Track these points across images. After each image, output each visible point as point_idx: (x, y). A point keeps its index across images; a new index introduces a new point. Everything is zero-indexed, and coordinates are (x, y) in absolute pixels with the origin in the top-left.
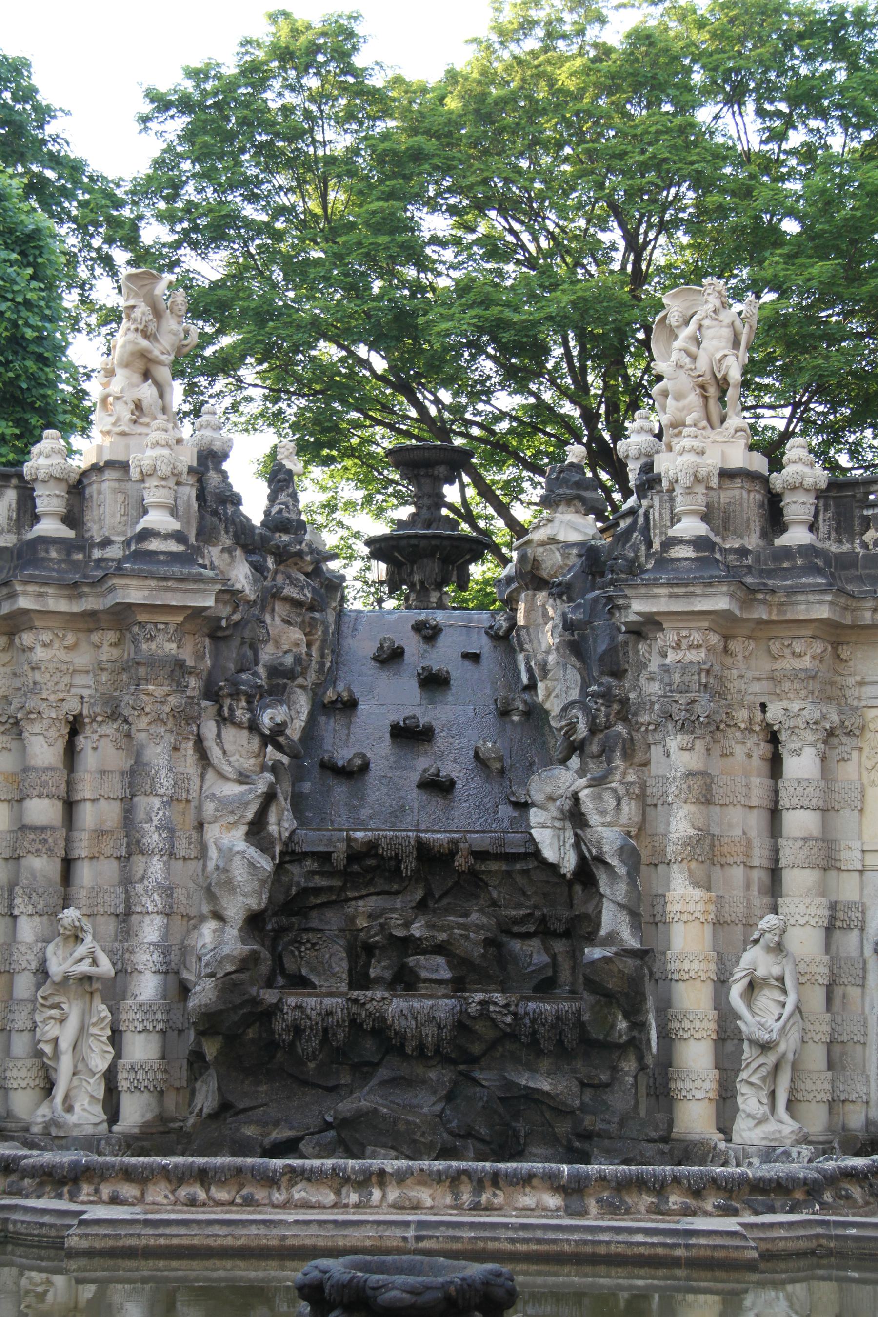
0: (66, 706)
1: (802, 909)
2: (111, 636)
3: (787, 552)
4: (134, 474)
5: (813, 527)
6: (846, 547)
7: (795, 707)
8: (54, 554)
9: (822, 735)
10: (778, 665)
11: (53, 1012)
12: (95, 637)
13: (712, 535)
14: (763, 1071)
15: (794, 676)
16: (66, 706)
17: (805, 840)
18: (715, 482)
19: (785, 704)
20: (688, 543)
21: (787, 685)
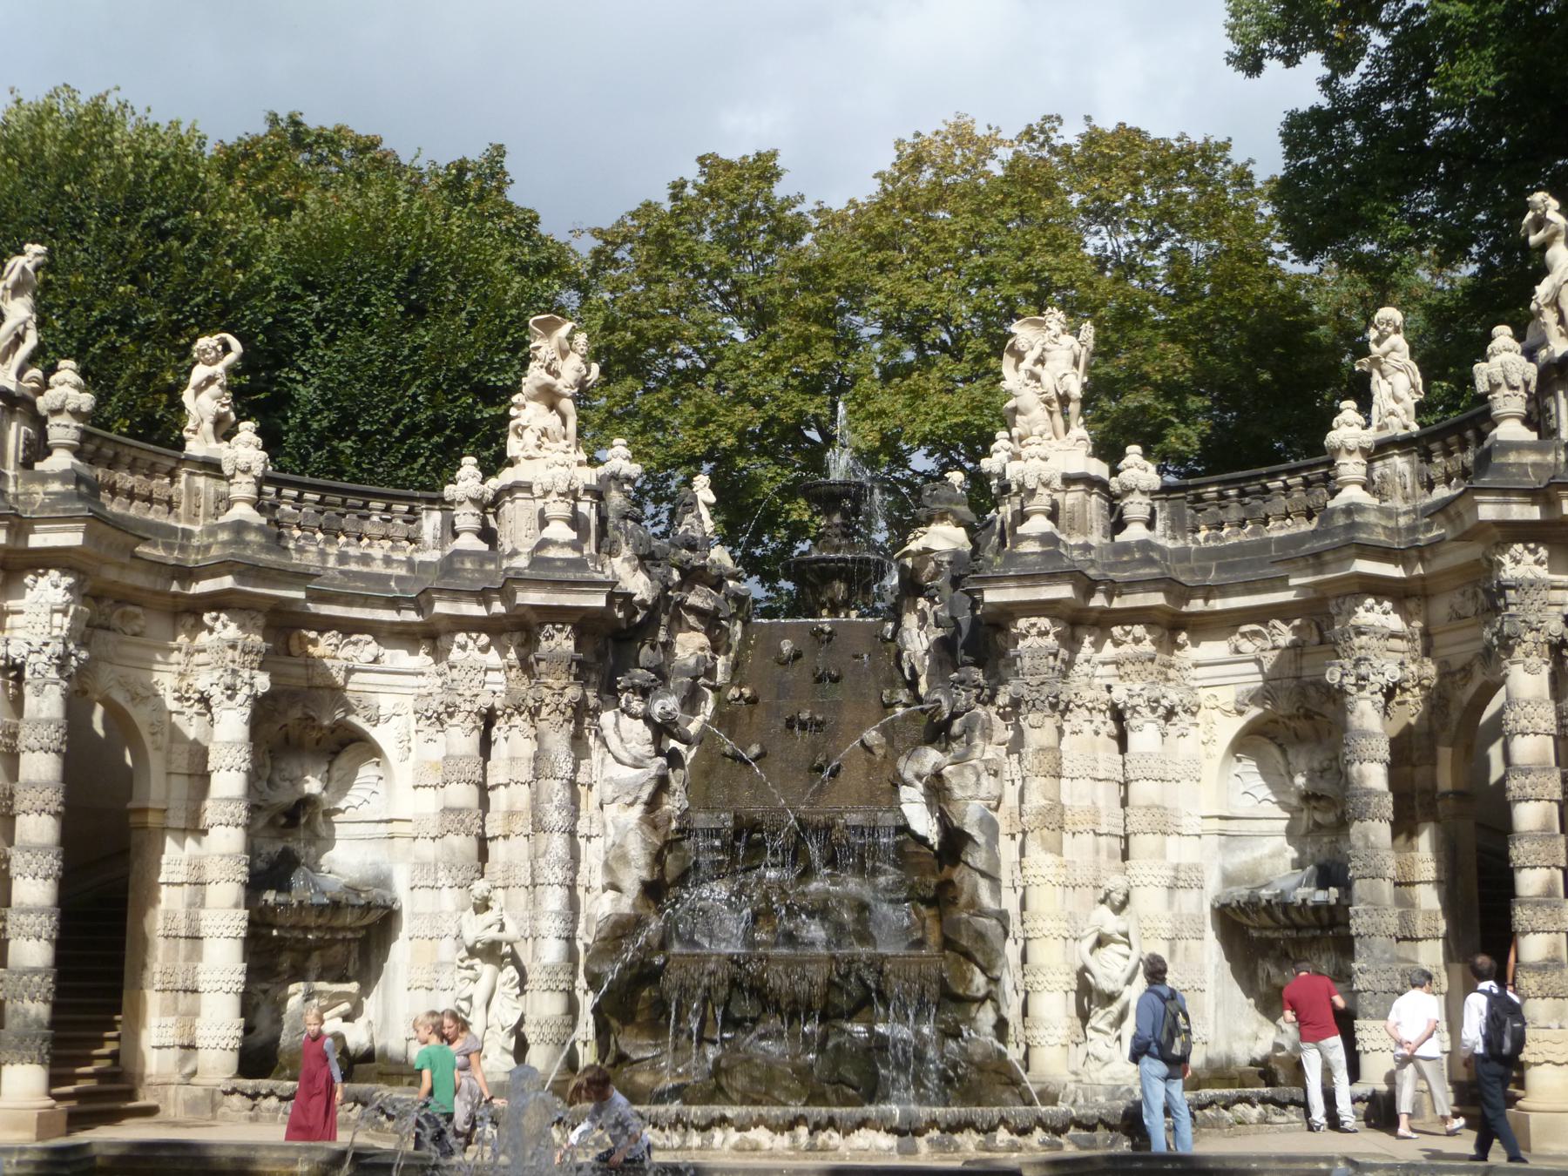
0: (479, 701)
1: (1146, 871)
2: (518, 637)
3: (1126, 548)
4: (537, 491)
5: (1150, 525)
6: (1180, 543)
7: (1137, 687)
8: (468, 565)
9: (1161, 711)
10: (1122, 649)
11: (470, 973)
12: (504, 638)
13: (1057, 532)
14: (1110, 1018)
15: (1137, 660)
16: (479, 701)
17: (1148, 808)
18: (1057, 483)
19: (1128, 684)
20: (1034, 538)
21: (1129, 668)
